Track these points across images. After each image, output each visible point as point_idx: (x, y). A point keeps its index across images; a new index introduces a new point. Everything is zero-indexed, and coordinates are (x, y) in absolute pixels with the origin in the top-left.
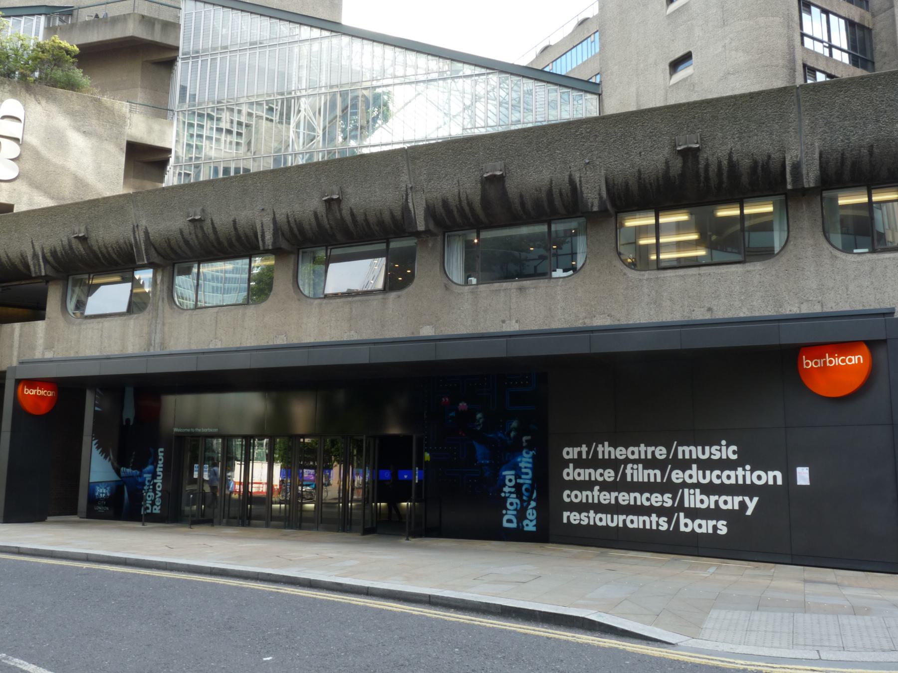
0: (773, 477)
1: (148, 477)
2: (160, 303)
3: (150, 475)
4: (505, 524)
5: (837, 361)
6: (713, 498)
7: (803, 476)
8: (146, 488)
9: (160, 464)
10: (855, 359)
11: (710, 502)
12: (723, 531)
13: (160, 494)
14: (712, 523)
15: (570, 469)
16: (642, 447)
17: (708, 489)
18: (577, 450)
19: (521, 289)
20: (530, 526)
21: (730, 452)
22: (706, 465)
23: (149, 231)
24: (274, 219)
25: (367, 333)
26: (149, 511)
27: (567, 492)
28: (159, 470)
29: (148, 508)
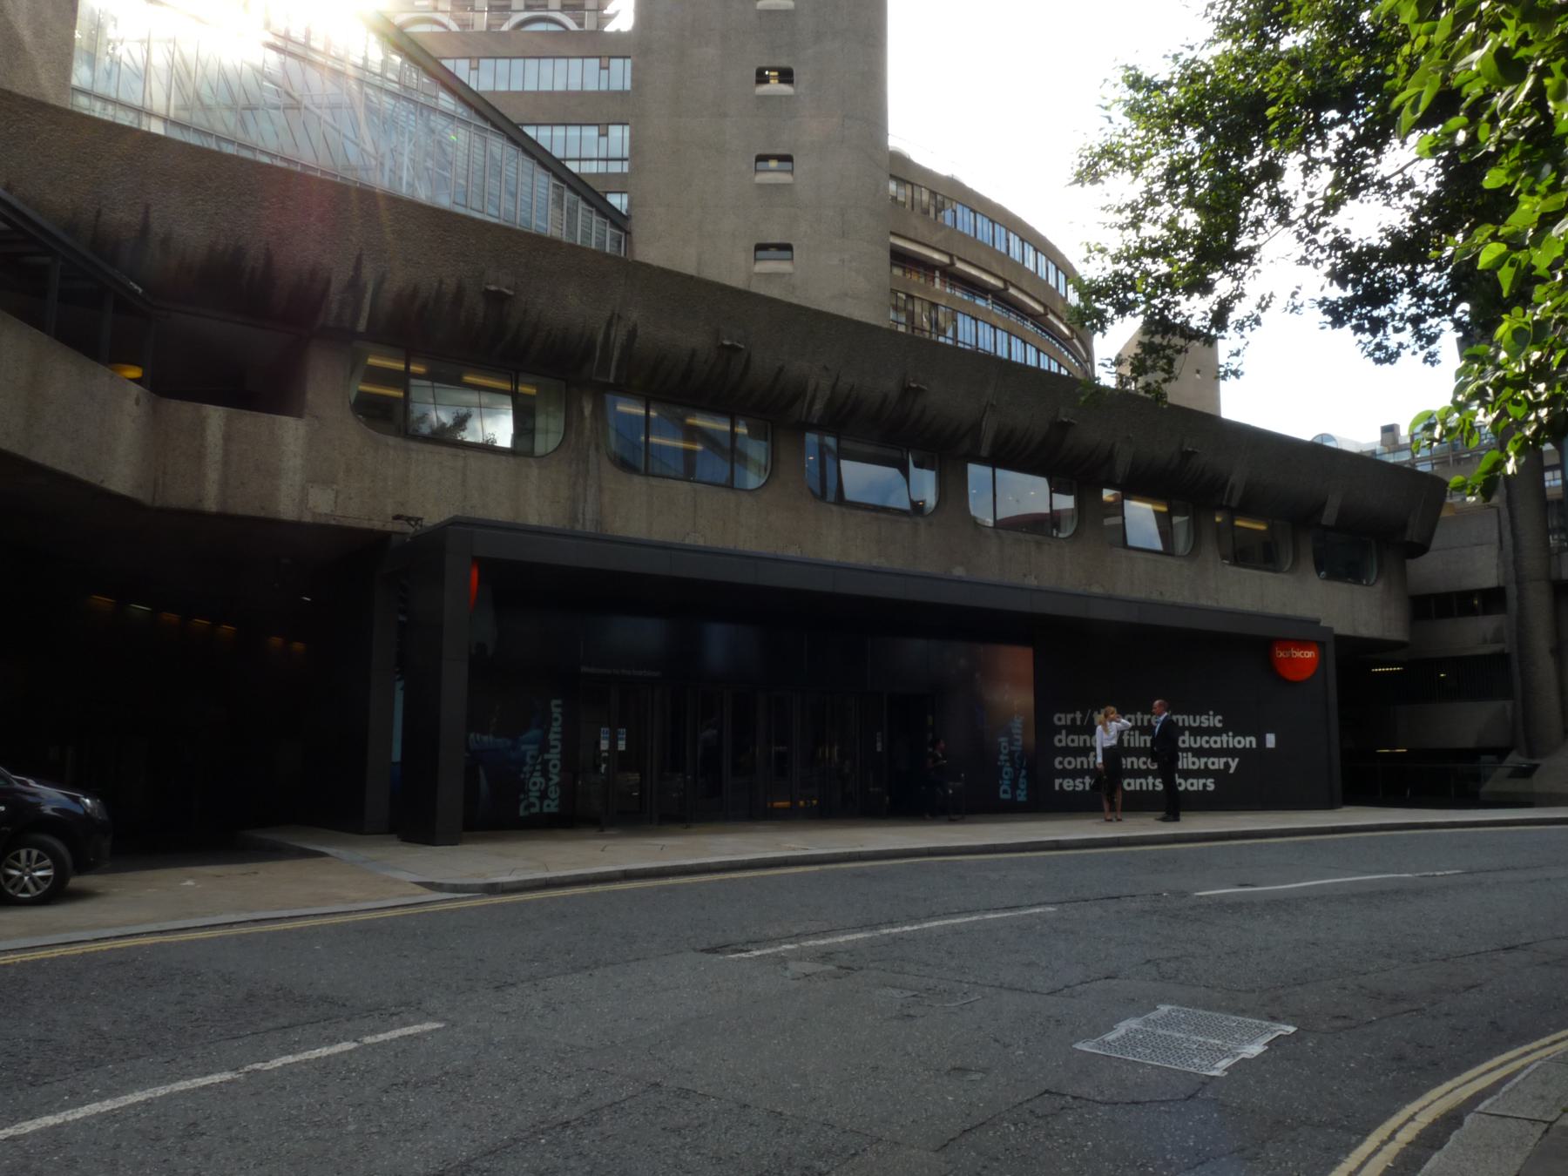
0: (1249, 741)
1: (530, 750)
2: (592, 452)
3: (535, 747)
4: (1003, 796)
5: (1299, 654)
6: (1203, 760)
7: (1271, 741)
8: (526, 769)
9: (556, 727)
10: (1309, 654)
11: (1200, 763)
12: (1211, 787)
13: (556, 779)
14: (1202, 781)
15: (1063, 736)
16: (1139, 715)
17: (1199, 753)
18: (1070, 716)
19: (1039, 544)
20: (1022, 796)
21: (1216, 721)
22: (1198, 732)
23: (640, 332)
24: (834, 386)
25: (896, 561)
26: (535, 810)
27: (1058, 759)
28: (554, 737)
29: (533, 805)
